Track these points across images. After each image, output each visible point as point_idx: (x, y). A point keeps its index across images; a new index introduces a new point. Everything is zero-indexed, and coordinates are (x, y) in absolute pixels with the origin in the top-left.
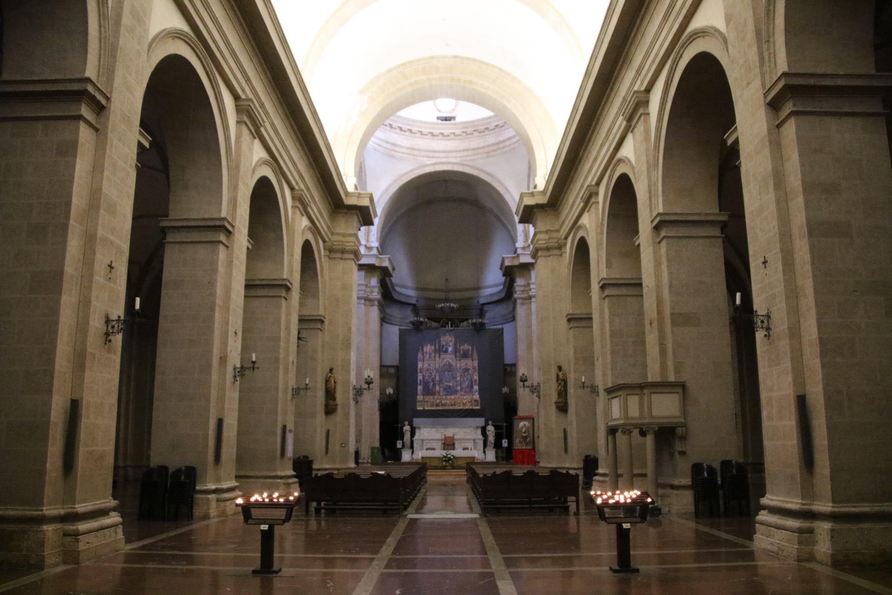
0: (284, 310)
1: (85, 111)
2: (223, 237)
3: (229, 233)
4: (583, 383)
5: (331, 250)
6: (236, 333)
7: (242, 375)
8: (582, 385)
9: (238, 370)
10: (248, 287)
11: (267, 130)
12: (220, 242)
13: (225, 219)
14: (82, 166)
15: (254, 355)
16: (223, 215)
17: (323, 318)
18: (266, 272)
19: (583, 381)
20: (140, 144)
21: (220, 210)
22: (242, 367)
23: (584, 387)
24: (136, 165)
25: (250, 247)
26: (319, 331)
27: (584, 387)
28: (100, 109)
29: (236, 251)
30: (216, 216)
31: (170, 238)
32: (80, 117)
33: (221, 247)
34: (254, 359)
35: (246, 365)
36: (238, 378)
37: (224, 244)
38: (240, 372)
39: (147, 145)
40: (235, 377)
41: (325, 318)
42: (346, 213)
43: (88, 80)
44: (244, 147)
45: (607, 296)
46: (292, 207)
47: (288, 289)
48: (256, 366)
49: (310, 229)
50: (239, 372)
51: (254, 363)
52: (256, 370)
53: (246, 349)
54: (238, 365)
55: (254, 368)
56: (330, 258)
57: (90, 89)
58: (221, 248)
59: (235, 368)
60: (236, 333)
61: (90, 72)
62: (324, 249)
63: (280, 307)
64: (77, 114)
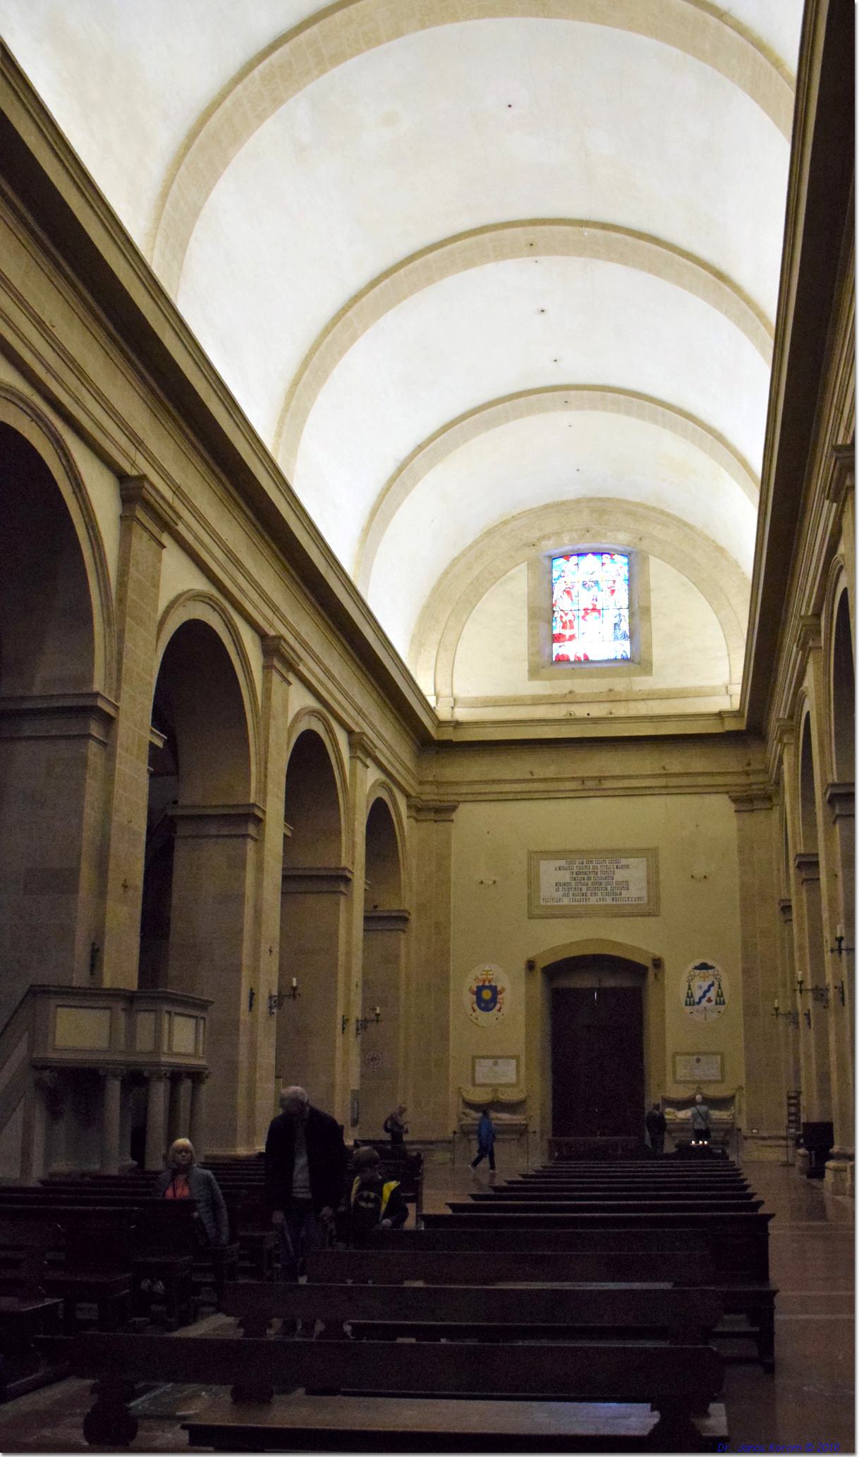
0: (342, 908)
1: (95, 729)
2: (251, 830)
3: (259, 821)
4: (777, 1009)
5: (419, 810)
6: (271, 951)
7: (280, 1005)
8: (774, 1012)
9: (276, 998)
10: (285, 878)
11: (308, 667)
12: (248, 836)
13: (254, 805)
14: (93, 787)
15: (294, 980)
16: (252, 801)
17: (407, 915)
18: (312, 860)
19: (776, 1006)
20: (152, 745)
21: (248, 793)
22: (280, 995)
23: (777, 1015)
24: (148, 770)
25: (289, 834)
26: (400, 932)
27: (777, 1015)
28: (109, 721)
29: (268, 845)
30: (243, 802)
31: (183, 830)
32: (90, 736)
33: (249, 840)
34: (295, 985)
35: (284, 993)
36: (275, 1011)
37: (252, 838)
38: (277, 1002)
39: (160, 744)
40: (271, 1008)
41: (409, 914)
42: (437, 753)
43: (97, 695)
44: (276, 699)
45: (805, 880)
46: (351, 758)
47: (347, 881)
48: (297, 992)
49: (383, 785)
50: (275, 1001)
51: (295, 989)
52: (298, 997)
53: (284, 972)
54: (275, 993)
55: (294, 996)
56: (417, 820)
57: (101, 704)
58: (249, 841)
59: (271, 997)
60: (271, 951)
61: (98, 686)
62: (409, 807)
63: (338, 904)
64: (85, 733)
